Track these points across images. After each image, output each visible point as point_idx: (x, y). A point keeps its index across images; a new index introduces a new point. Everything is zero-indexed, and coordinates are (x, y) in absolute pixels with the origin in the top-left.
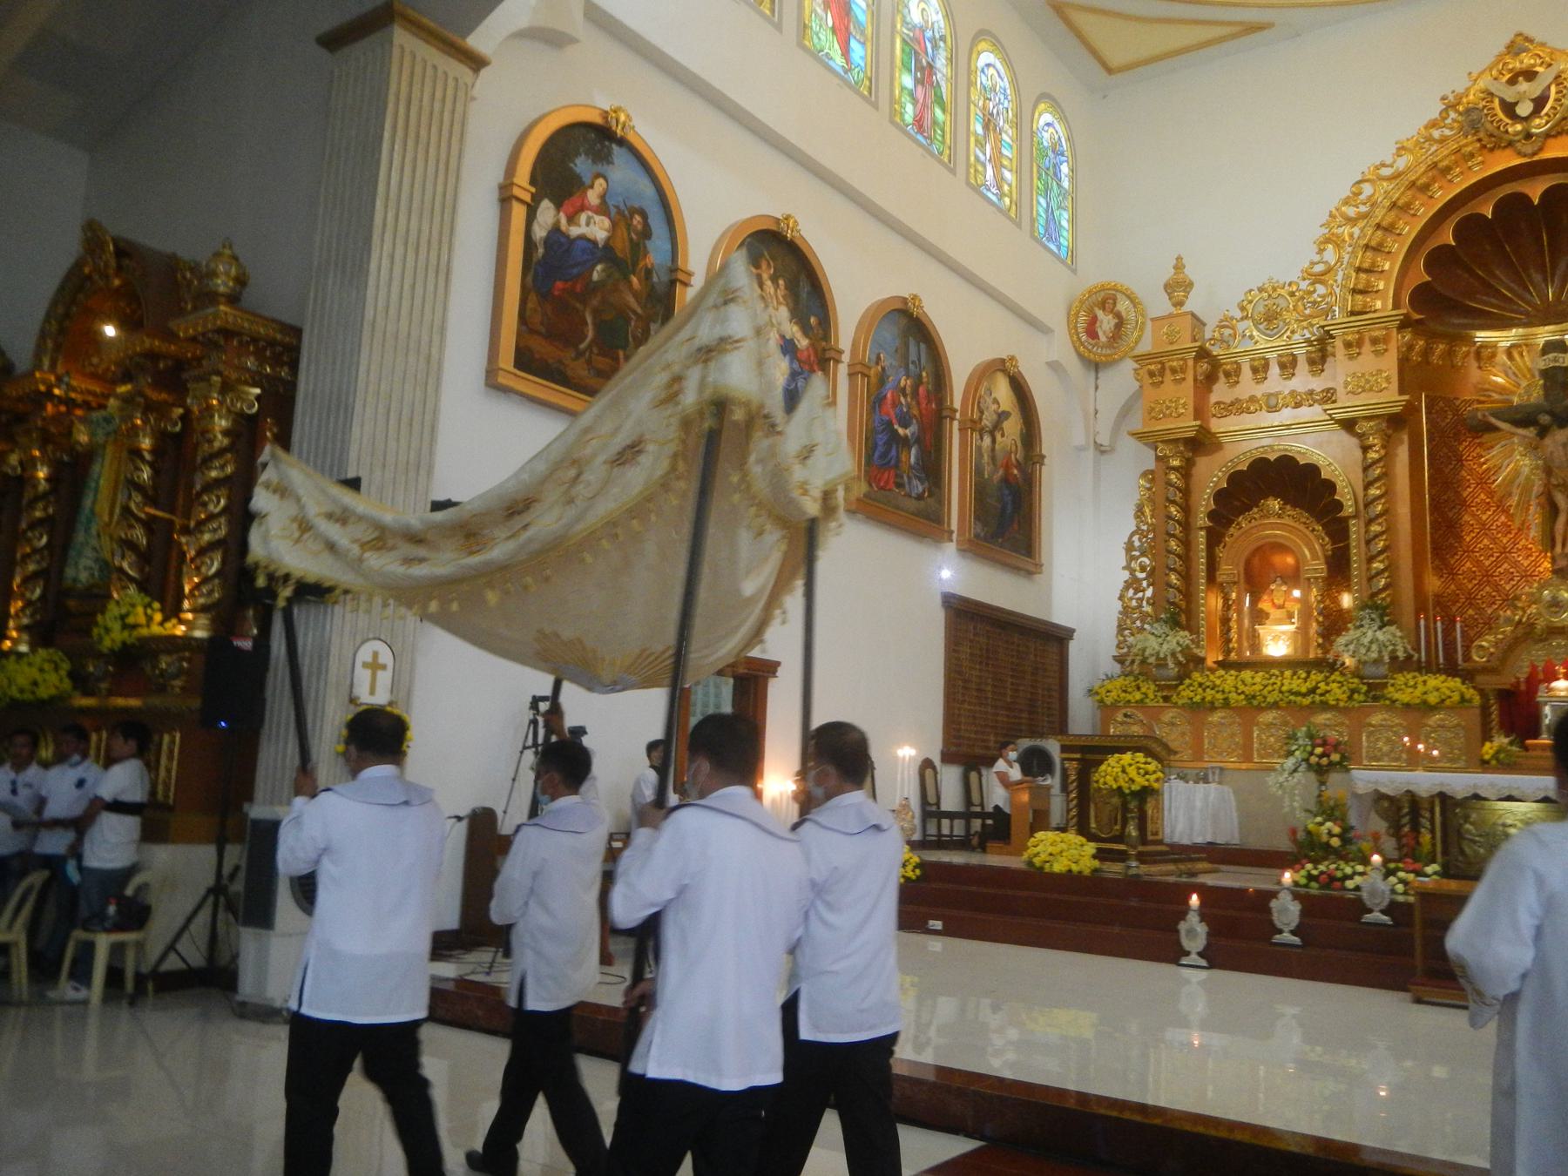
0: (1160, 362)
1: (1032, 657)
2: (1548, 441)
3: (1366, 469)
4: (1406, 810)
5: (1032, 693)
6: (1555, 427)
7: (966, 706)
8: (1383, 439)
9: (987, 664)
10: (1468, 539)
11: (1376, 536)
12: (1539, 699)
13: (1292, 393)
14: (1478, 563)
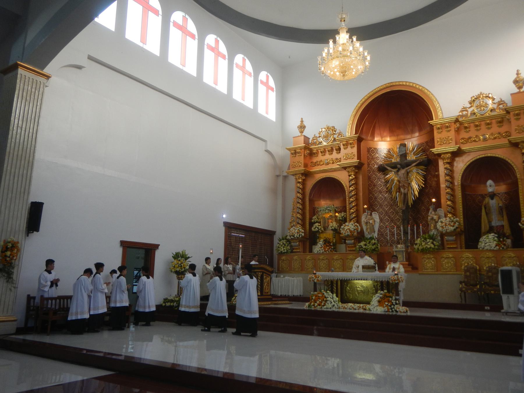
0: (294, 150)
1: (260, 241)
2: (399, 173)
3: (349, 182)
4: (330, 284)
6: (401, 169)
10: (381, 202)
12: (393, 250)
13: (332, 159)
14: (384, 209)
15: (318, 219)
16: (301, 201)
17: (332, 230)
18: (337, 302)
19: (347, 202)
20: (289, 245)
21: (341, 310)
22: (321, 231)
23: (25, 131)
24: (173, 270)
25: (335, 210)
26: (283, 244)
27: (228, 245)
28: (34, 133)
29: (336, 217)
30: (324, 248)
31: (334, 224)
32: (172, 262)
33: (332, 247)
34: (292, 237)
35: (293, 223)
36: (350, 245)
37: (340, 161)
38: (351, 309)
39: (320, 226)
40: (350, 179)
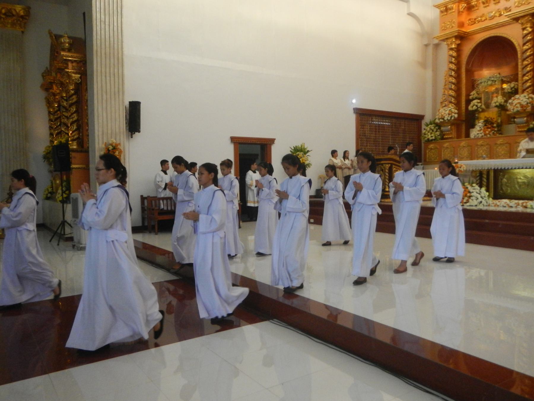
1: (403, 127)
3: (524, 37)
4: (478, 175)
5: (403, 140)
7: (368, 147)
8: (530, 24)
9: (379, 132)
11: (527, 66)
13: (499, 9)
15: (478, 94)
16: (454, 74)
17: (496, 106)
18: (487, 198)
19: (520, 67)
20: (438, 130)
21: (492, 208)
22: (480, 110)
23: (109, 25)
25: (502, 80)
26: (431, 129)
27: (361, 135)
28: (119, 26)
29: (503, 89)
30: (484, 131)
31: (499, 99)
33: (496, 129)
34: (441, 120)
35: (445, 103)
36: (520, 124)
37: (510, 11)
38: (505, 207)
39: (481, 102)
40: (524, 35)
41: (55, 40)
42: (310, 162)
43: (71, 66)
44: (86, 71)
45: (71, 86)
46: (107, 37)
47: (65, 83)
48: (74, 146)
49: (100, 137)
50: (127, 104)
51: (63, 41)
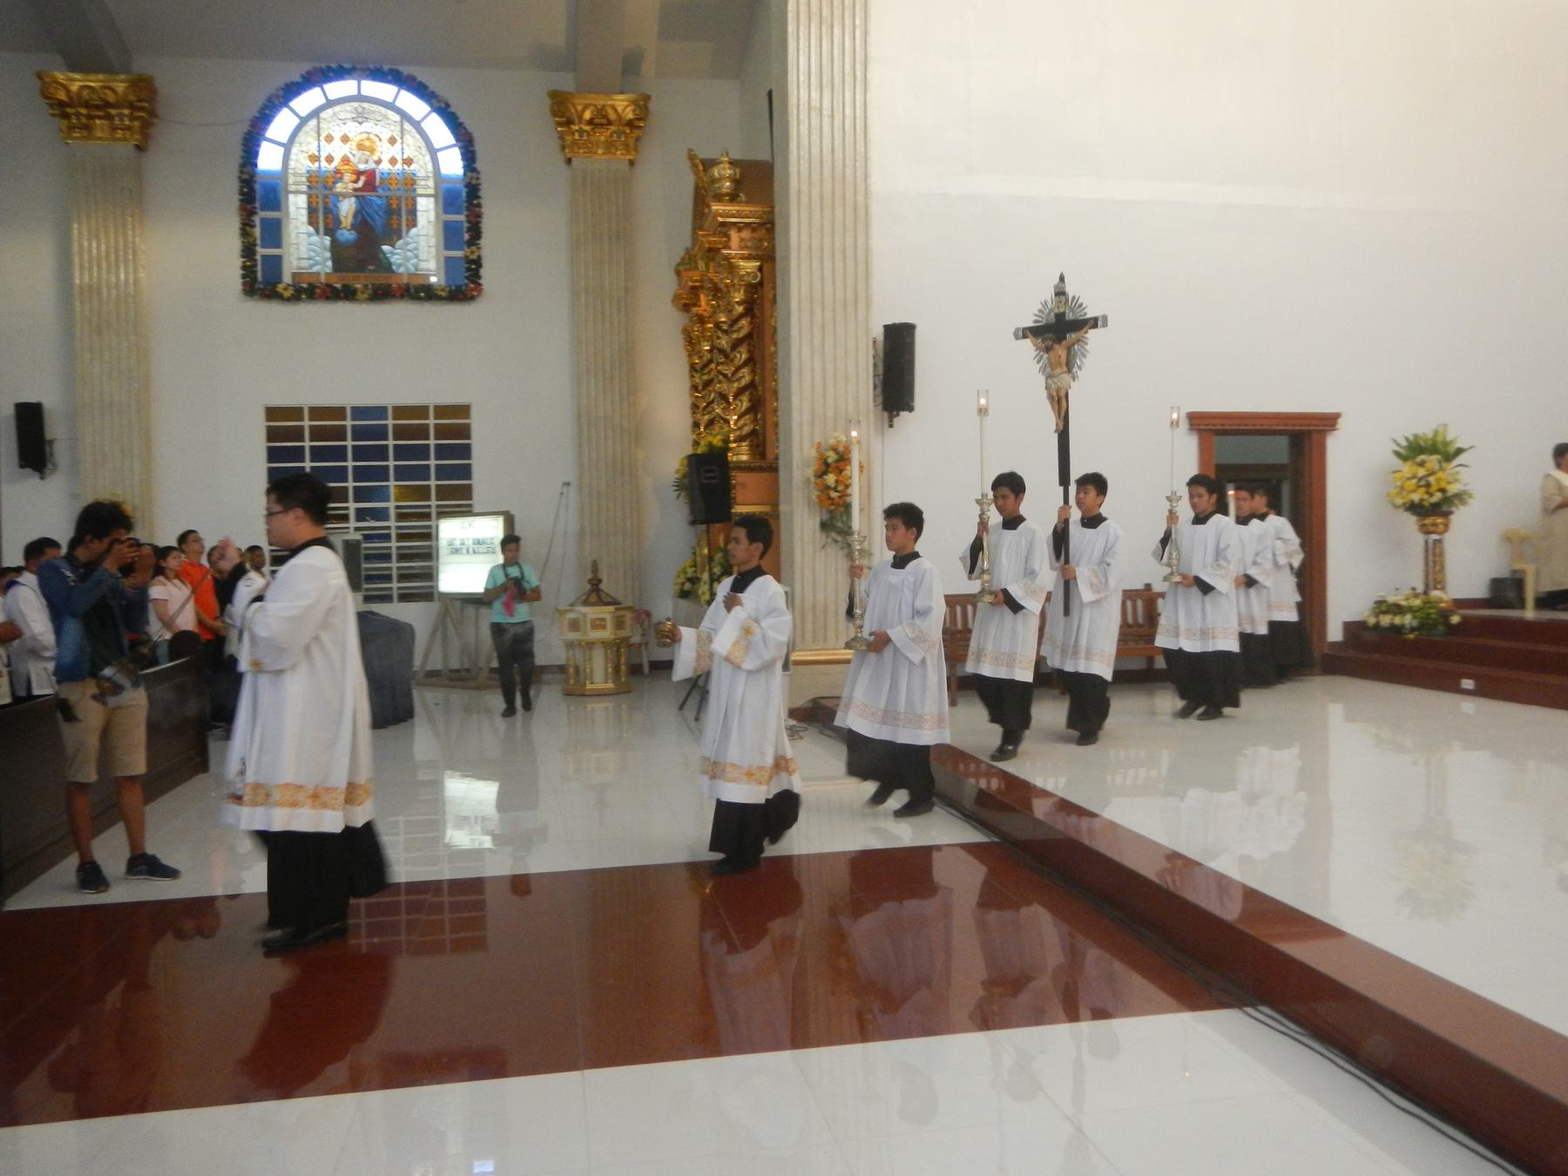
23: (832, 117)
24: (1399, 501)
28: (858, 115)
32: (1395, 472)
41: (702, 174)
42: (1467, 488)
43: (738, 240)
44: (773, 248)
45: (736, 294)
46: (827, 150)
47: (722, 286)
48: (741, 454)
49: (806, 430)
50: (878, 332)
51: (716, 174)
